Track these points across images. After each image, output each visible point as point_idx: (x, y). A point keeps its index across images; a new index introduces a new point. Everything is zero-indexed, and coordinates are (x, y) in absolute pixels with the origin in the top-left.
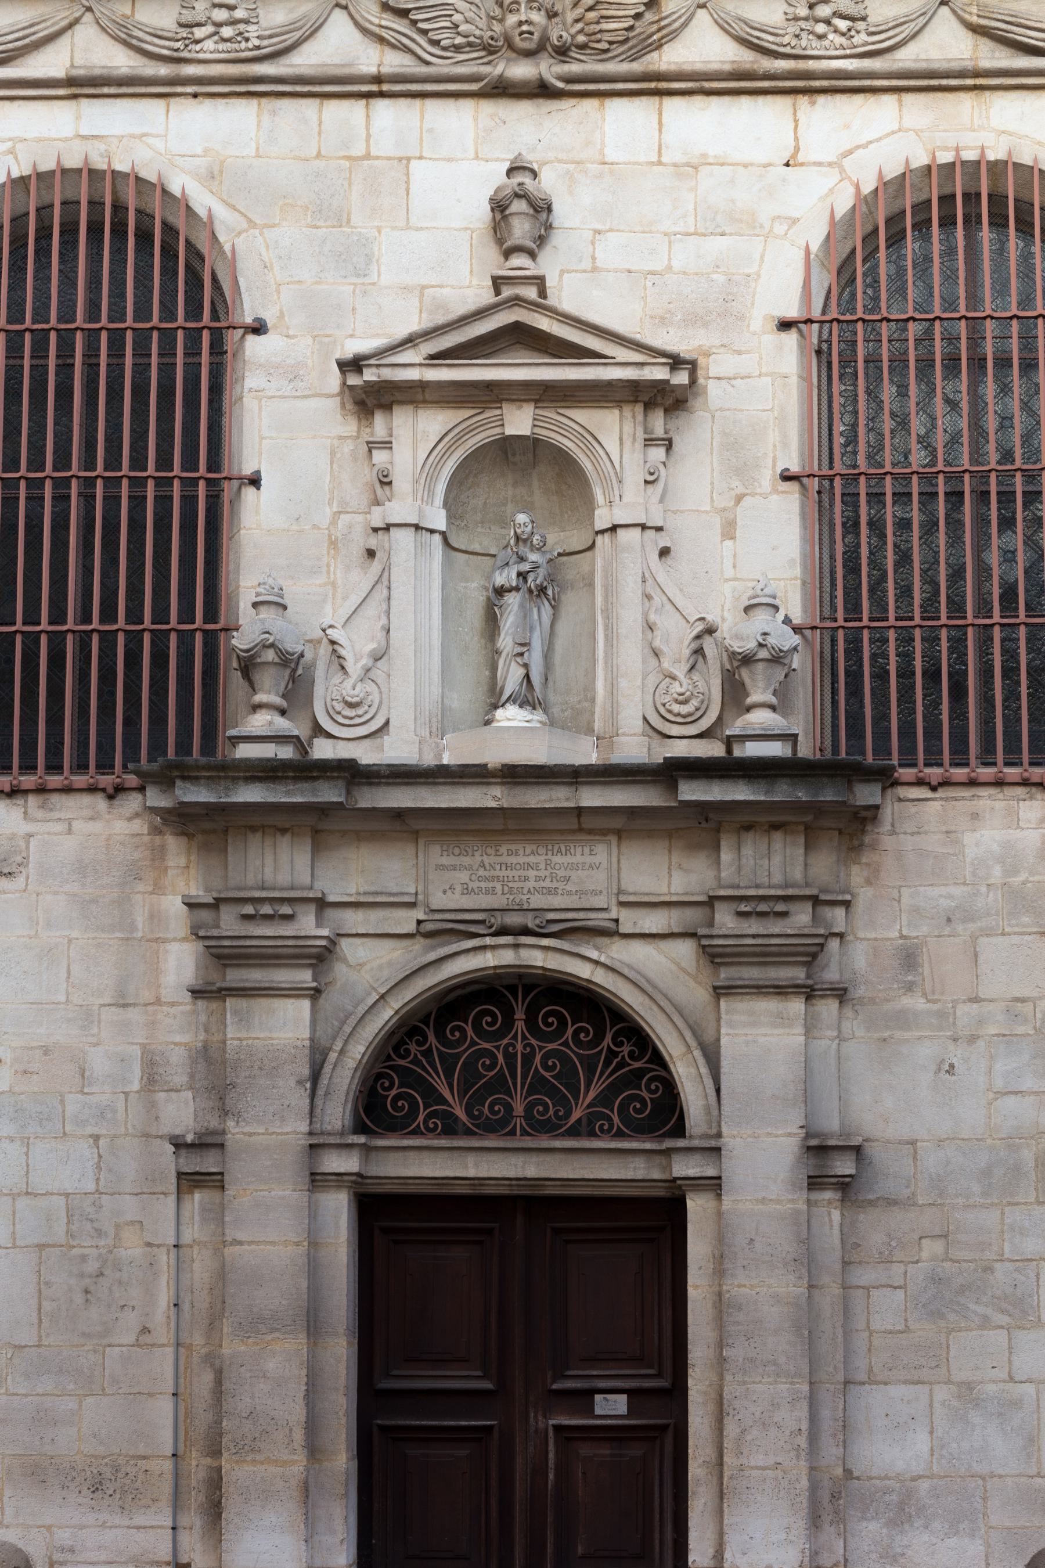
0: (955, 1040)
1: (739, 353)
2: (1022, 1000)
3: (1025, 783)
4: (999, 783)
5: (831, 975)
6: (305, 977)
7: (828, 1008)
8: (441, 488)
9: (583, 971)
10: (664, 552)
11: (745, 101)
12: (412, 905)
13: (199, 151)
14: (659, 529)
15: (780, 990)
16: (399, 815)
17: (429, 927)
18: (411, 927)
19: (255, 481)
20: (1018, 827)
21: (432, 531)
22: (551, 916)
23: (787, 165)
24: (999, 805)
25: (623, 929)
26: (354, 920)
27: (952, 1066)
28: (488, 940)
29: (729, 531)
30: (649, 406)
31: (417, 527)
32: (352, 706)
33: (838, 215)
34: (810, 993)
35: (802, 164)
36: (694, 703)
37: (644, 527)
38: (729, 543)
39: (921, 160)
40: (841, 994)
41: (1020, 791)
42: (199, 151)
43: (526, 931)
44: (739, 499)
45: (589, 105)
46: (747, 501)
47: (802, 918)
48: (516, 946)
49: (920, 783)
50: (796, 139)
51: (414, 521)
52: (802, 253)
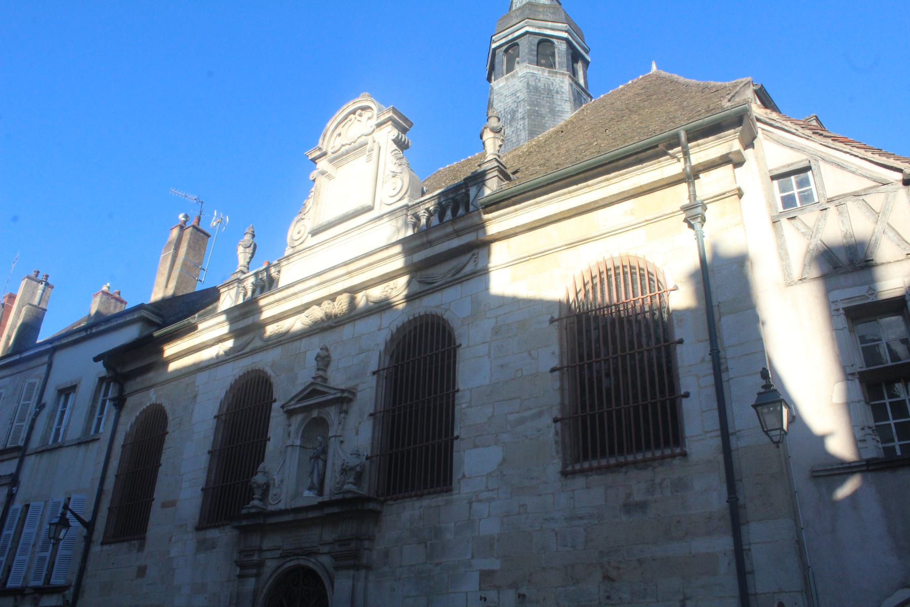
0: (395, 580)
1: (364, 383)
2: (412, 566)
3: (416, 496)
4: (410, 497)
5: (364, 561)
6: (254, 571)
7: (363, 573)
8: (300, 434)
9: (311, 565)
10: (342, 442)
11: (371, 317)
12: (279, 549)
14: (340, 436)
15: (348, 568)
16: (277, 524)
17: (282, 555)
18: (278, 556)
19: (269, 439)
20: (414, 510)
21: (297, 446)
22: (307, 549)
23: (379, 330)
24: (410, 503)
25: (321, 552)
26: (268, 554)
27: (394, 589)
28: (292, 558)
29: (357, 434)
30: (342, 403)
31: (292, 446)
32: (275, 495)
33: (388, 341)
34: (357, 567)
35: (382, 329)
36: (340, 484)
37: (336, 436)
38: (357, 436)
39: (406, 319)
40: (368, 568)
41: (415, 498)
43: (300, 555)
44: (360, 423)
45: (341, 327)
46: (362, 424)
47: (353, 545)
48: (298, 559)
49: (391, 499)
50: (381, 323)
51: (291, 444)
52: (379, 353)
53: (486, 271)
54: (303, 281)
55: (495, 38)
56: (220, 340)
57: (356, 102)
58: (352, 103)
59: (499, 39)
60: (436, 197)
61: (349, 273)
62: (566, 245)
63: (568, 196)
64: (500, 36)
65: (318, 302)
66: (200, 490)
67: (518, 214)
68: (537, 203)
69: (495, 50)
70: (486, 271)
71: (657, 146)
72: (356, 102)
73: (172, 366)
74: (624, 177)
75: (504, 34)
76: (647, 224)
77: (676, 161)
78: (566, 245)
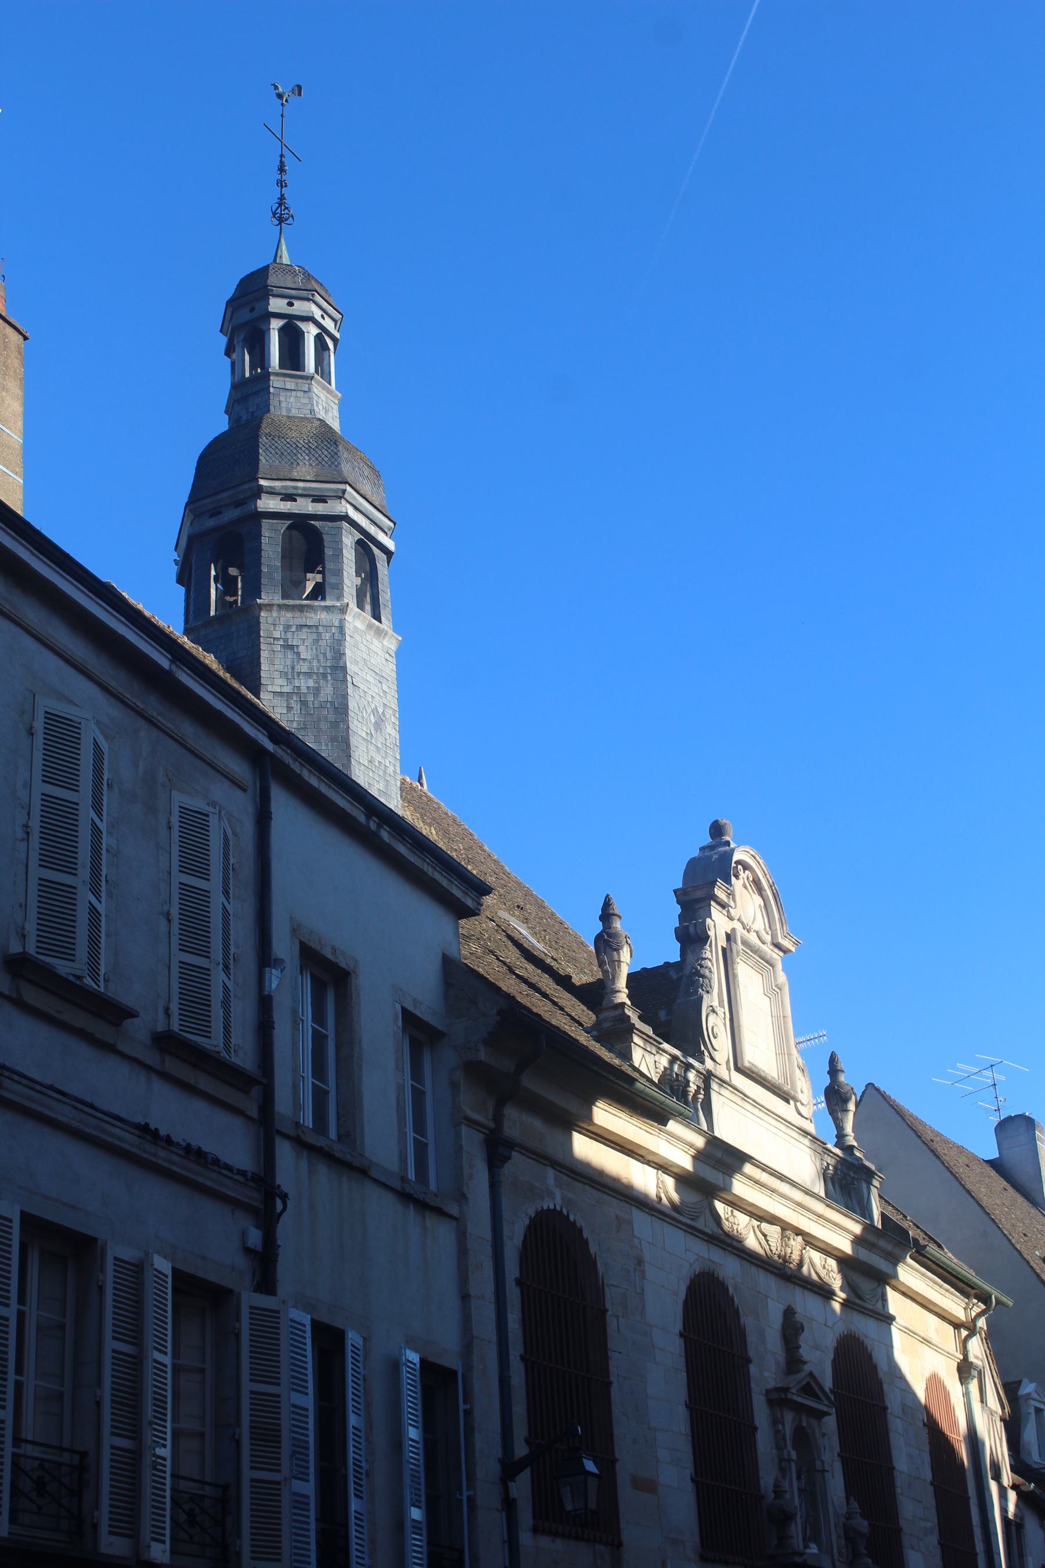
13: (731, 1276)
42: (731, 1276)
53: (889, 1321)
54: (794, 1186)
55: (350, 493)
56: (662, 1166)
57: (755, 858)
58: (753, 853)
59: (351, 501)
60: (838, 1158)
61: (820, 1216)
62: (923, 1339)
63: (931, 1284)
64: (355, 498)
65: (786, 1227)
66: (690, 1480)
67: (913, 1274)
68: (923, 1275)
69: (346, 518)
70: (889, 1321)
71: (973, 1288)
72: (755, 858)
73: (583, 1147)
74: (947, 1294)
75: (361, 504)
76: (906, 1333)
77: (964, 1306)
78: (923, 1339)
